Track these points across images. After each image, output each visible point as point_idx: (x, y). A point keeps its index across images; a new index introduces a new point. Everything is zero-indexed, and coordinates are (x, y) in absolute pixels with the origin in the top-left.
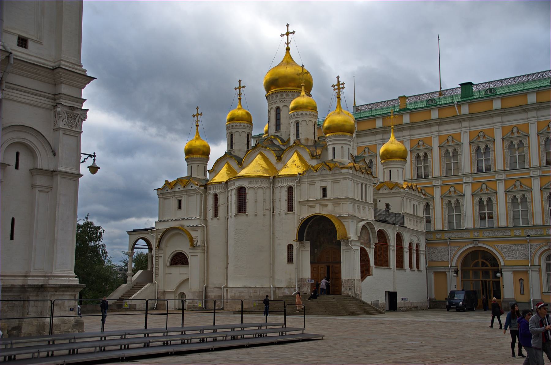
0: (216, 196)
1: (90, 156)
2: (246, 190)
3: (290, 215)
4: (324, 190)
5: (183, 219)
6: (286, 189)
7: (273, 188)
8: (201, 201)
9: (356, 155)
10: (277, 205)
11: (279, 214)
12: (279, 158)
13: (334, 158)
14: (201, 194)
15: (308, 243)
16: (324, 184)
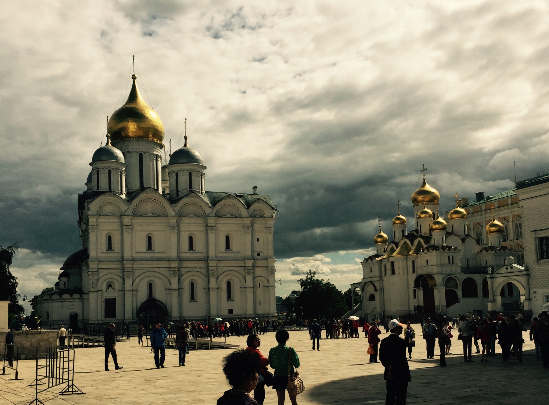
0: (385, 265)
1: (279, 280)
2: (394, 263)
3: (414, 274)
4: (427, 261)
5: (372, 277)
6: (411, 261)
7: (407, 260)
8: (379, 267)
9: (467, 234)
10: (409, 269)
11: (410, 274)
12: (412, 244)
13: (434, 244)
14: (379, 265)
15: (422, 288)
16: (427, 258)
